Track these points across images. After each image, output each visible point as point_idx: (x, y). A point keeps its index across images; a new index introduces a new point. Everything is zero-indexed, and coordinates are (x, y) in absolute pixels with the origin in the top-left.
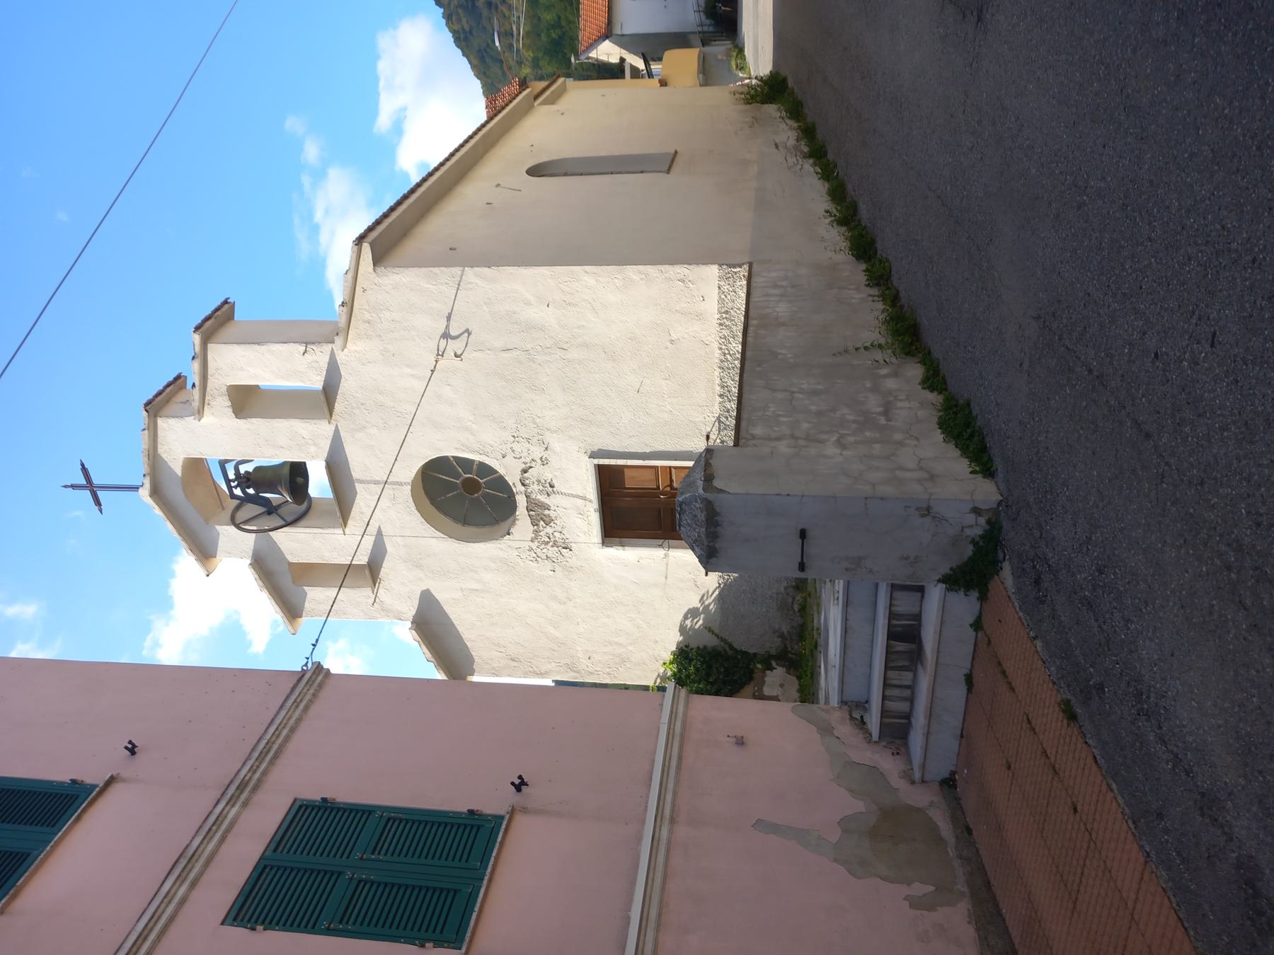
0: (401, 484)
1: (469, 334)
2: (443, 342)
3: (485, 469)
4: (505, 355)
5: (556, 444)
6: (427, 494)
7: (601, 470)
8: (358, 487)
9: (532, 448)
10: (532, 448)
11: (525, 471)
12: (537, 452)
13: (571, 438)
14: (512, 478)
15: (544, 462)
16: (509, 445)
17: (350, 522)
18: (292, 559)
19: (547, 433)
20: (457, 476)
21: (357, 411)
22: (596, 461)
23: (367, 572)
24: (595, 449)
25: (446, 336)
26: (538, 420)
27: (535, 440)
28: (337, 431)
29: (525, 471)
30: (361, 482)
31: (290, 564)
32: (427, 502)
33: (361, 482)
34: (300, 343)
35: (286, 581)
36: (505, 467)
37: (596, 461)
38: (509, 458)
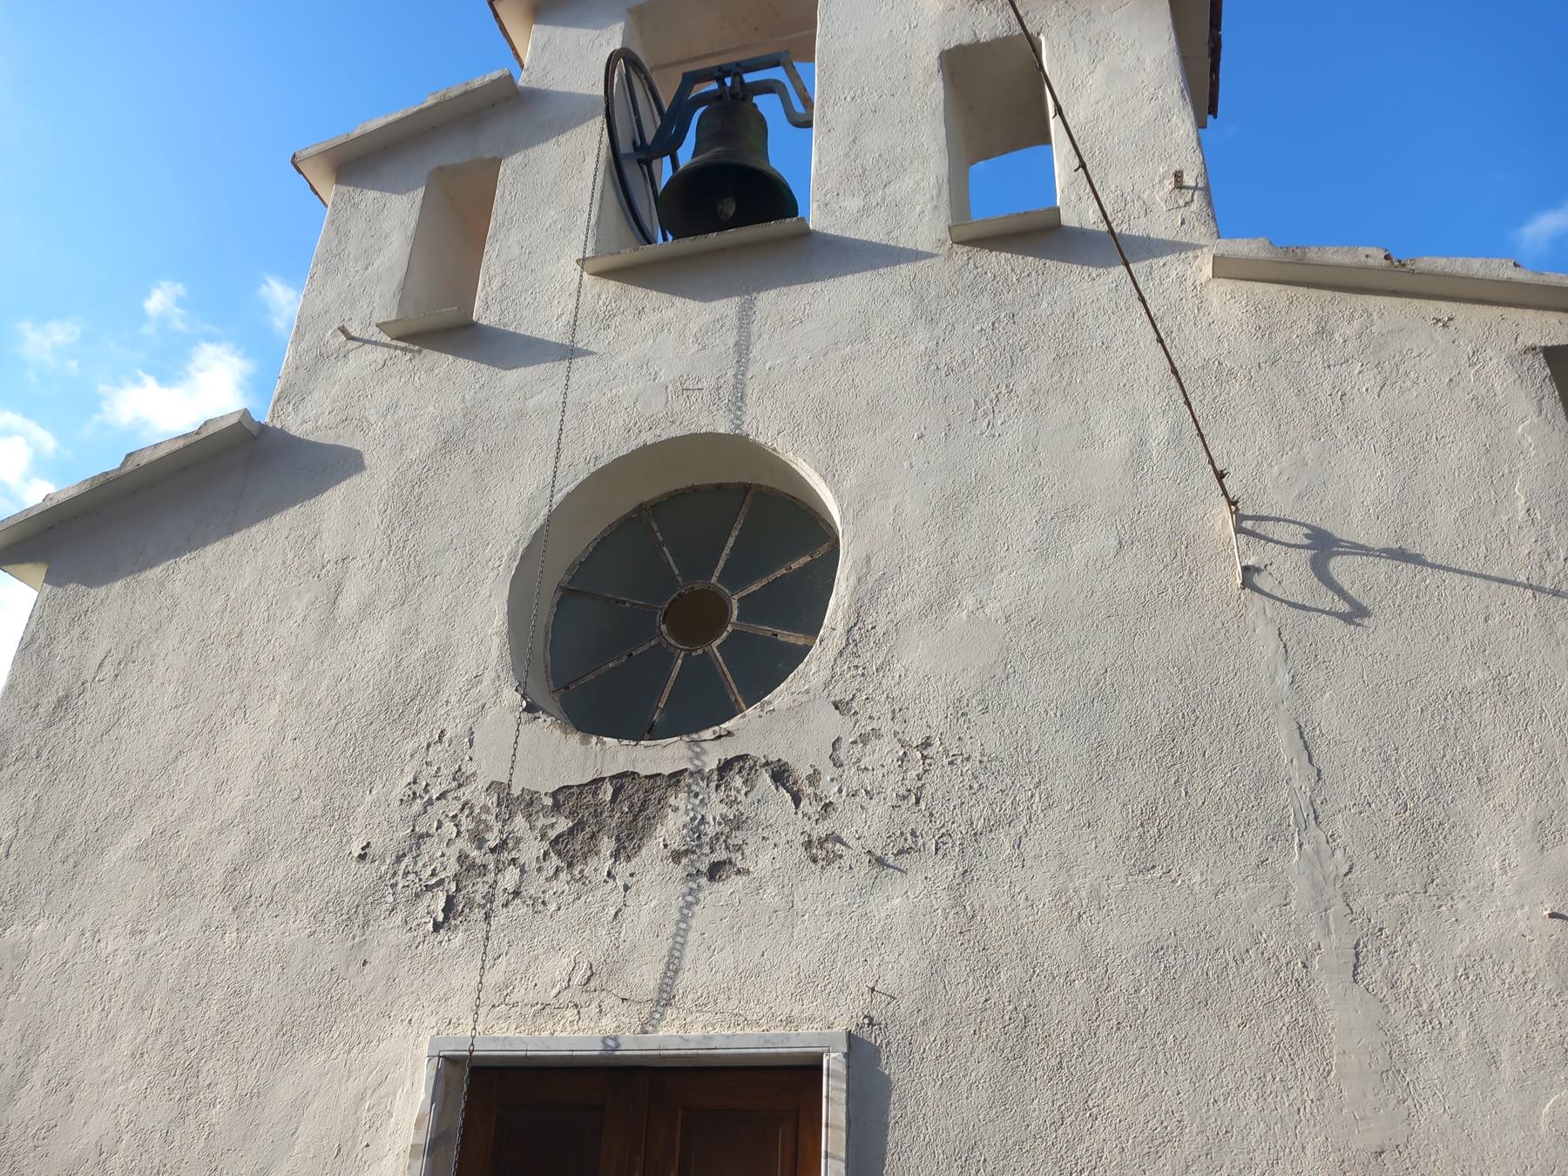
0: (739, 398)
1: (1347, 618)
2: (1298, 535)
3: (765, 668)
4: (1283, 737)
5: (896, 900)
6: (676, 497)
7: (801, 1075)
8: (727, 307)
9: (878, 808)
10: (878, 808)
11: (781, 775)
12: (864, 825)
13: (936, 967)
14: (752, 730)
15: (821, 850)
16: (886, 727)
17: (612, 286)
18: (506, 170)
19: (948, 870)
20: (734, 578)
21: (986, 301)
22: (834, 1063)
23: (449, 313)
24: (892, 1067)
25: (1322, 545)
26: (1004, 840)
27: (915, 820)
28: (915, 256)
29: (781, 775)
30: (745, 316)
31: (495, 164)
32: (651, 492)
33: (745, 316)
34: (1206, 174)
35: (452, 153)
36: (796, 710)
37: (834, 1063)
38: (831, 724)
